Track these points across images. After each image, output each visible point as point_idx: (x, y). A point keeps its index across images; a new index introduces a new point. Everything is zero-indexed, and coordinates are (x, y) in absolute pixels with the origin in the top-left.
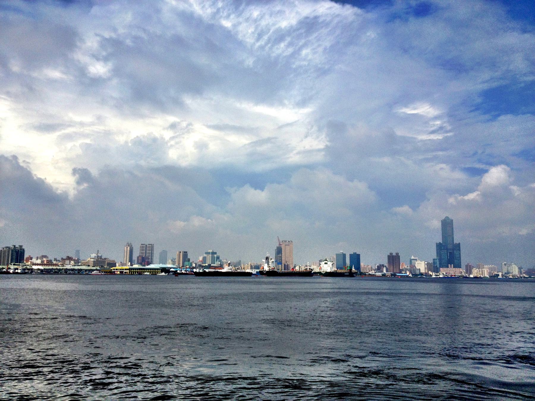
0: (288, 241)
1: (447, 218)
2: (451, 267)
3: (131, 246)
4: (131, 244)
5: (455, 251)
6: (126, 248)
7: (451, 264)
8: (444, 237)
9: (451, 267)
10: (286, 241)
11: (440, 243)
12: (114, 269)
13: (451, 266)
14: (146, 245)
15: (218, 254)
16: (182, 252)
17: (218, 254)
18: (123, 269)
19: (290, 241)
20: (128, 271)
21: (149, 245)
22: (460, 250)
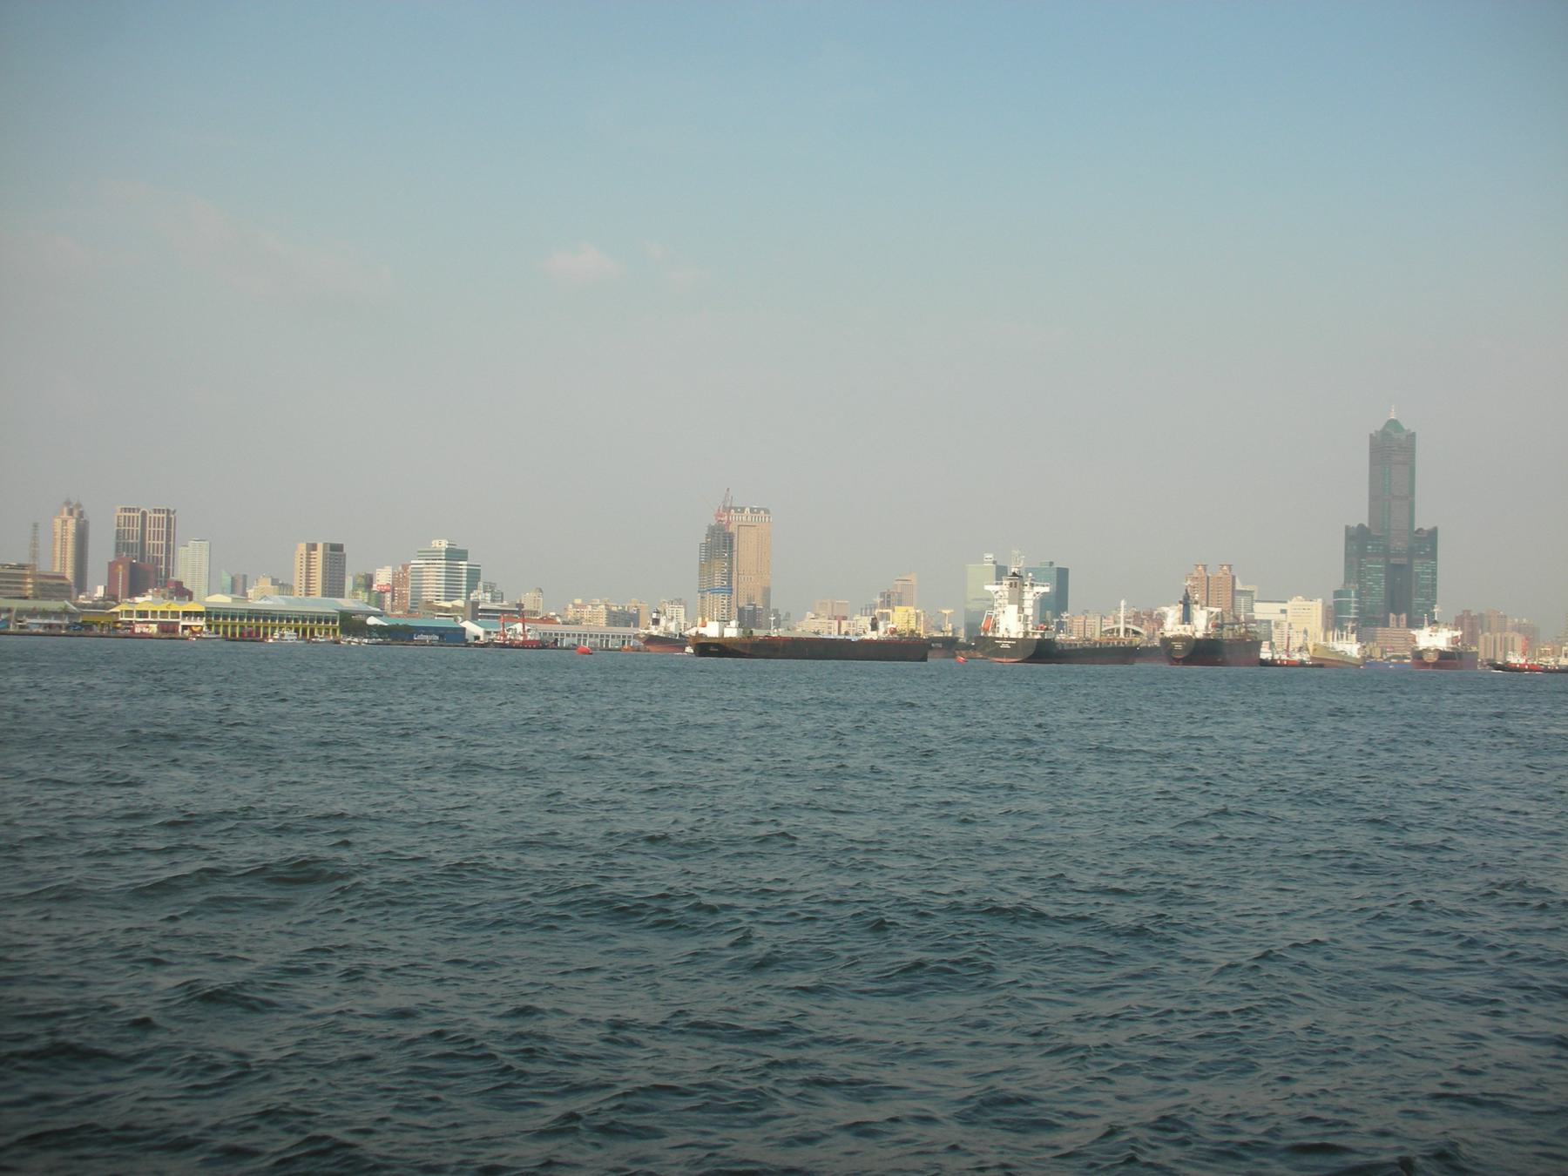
0: (752, 510)
1: (1393, 424)
2: (1398, 626)
3: (81, 514)
4: (79, 506)
5: (1416, 561)
6: (58, 522)
7: (1398, 613)
8: (1378, 498)
9: (1398, 626)
10: (743, 510)
11: (1361, 526)
12: (129, 613)
13: (1398, 620)
14: (144, 514)
15: (473, 559)
16: (320, 547)
17: (473, 559)
18: (175, 614)
19: (759, 510)
20: (202, 622)
21: (155, 511)
22: (1433, 555)
